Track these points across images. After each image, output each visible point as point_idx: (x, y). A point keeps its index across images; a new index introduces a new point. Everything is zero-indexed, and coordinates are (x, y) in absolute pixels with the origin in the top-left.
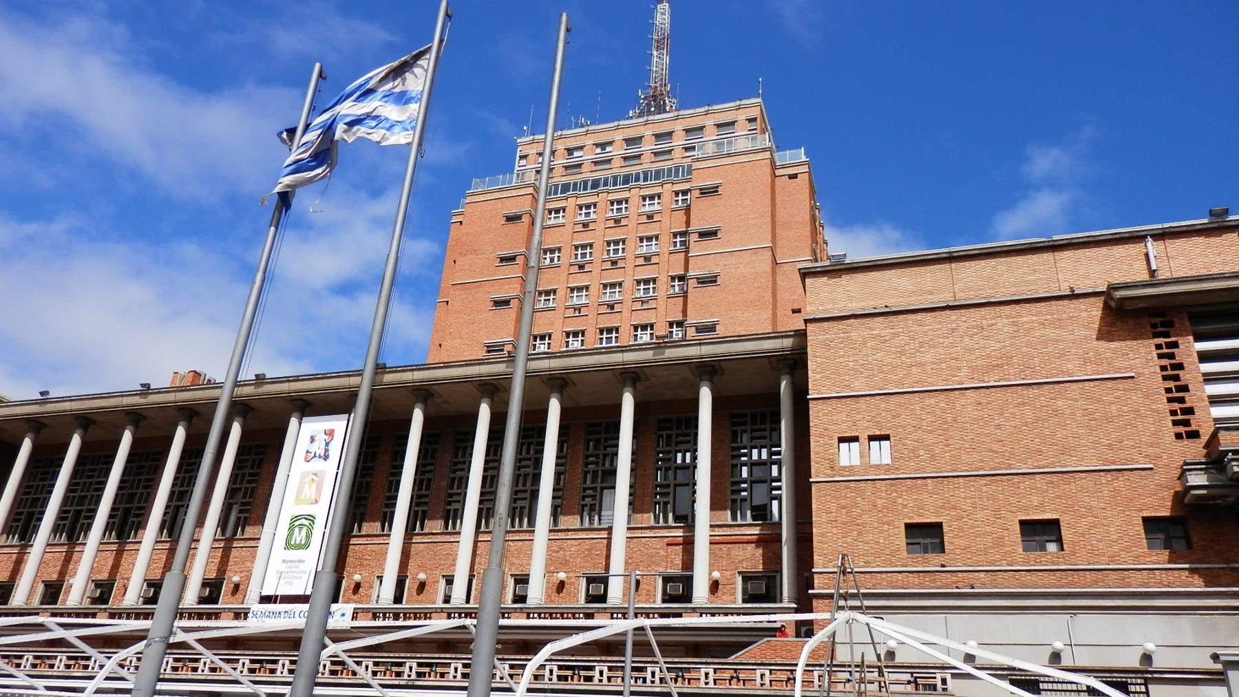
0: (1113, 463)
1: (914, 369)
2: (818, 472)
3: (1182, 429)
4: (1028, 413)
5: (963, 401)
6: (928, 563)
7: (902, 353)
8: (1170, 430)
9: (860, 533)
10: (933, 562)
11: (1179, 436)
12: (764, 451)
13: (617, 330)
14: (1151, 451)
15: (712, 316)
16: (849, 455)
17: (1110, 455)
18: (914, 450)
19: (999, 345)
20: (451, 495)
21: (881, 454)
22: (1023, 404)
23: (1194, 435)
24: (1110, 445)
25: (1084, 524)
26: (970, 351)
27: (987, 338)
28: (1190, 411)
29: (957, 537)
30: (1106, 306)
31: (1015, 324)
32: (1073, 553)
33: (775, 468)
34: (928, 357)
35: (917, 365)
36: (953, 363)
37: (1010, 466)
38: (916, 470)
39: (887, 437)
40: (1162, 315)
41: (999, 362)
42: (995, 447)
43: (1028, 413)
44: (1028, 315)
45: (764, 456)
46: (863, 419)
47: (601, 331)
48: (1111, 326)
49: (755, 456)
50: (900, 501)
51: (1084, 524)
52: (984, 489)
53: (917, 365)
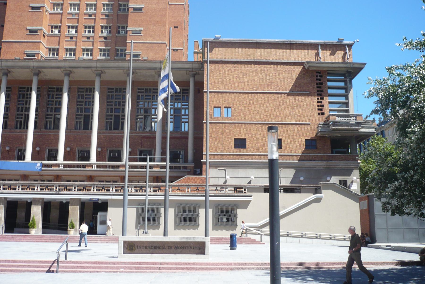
0: (299, 121)
1: (241, 84)
2: (207, 119)
3: (320, 112)
4: (276, 103)
5: (256, 97)
6: (240, 152)
7: (237, 77)
8: (317, 112)
9: (219, 141)
10: (243, 152)
11: (319, 114)
12: (180, 104)
13: (94, 27)
14: (310, 118)
15: (140, 26)
16: (216, 113)
17: (299, 119)
18: (239, 113)
19: (269, 78)
20: (47, 115)
21: (227, 113)
22: (275, 99)
23: (323, 114)
24: (299, 115)
25: (289, 140)
26: (261, 79)
27: (266, 75)
28: (323, 106)
29: (250, 143)
30: (304, 68)
31: (276, 71)
32: (284, 150)
33: (183, 111)
34: (246, 80)
35: (243, 82)
36: (254, 83)
37: (269, 121)
38: (239, 120)
39: (231, 108)
40: (320, 73)
41: (269, 84)
42: (265, 114)
43: (276, 103)
44: (280, 68)
45: (180, 106)
46: (223, 100)
47: (86, 27)
48: (305, 74)
49: (176, 106)
50: (233, 130)
51: (289, 140)
52: (260, 128)
53: (243, 82)
